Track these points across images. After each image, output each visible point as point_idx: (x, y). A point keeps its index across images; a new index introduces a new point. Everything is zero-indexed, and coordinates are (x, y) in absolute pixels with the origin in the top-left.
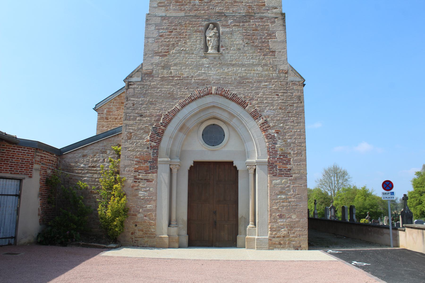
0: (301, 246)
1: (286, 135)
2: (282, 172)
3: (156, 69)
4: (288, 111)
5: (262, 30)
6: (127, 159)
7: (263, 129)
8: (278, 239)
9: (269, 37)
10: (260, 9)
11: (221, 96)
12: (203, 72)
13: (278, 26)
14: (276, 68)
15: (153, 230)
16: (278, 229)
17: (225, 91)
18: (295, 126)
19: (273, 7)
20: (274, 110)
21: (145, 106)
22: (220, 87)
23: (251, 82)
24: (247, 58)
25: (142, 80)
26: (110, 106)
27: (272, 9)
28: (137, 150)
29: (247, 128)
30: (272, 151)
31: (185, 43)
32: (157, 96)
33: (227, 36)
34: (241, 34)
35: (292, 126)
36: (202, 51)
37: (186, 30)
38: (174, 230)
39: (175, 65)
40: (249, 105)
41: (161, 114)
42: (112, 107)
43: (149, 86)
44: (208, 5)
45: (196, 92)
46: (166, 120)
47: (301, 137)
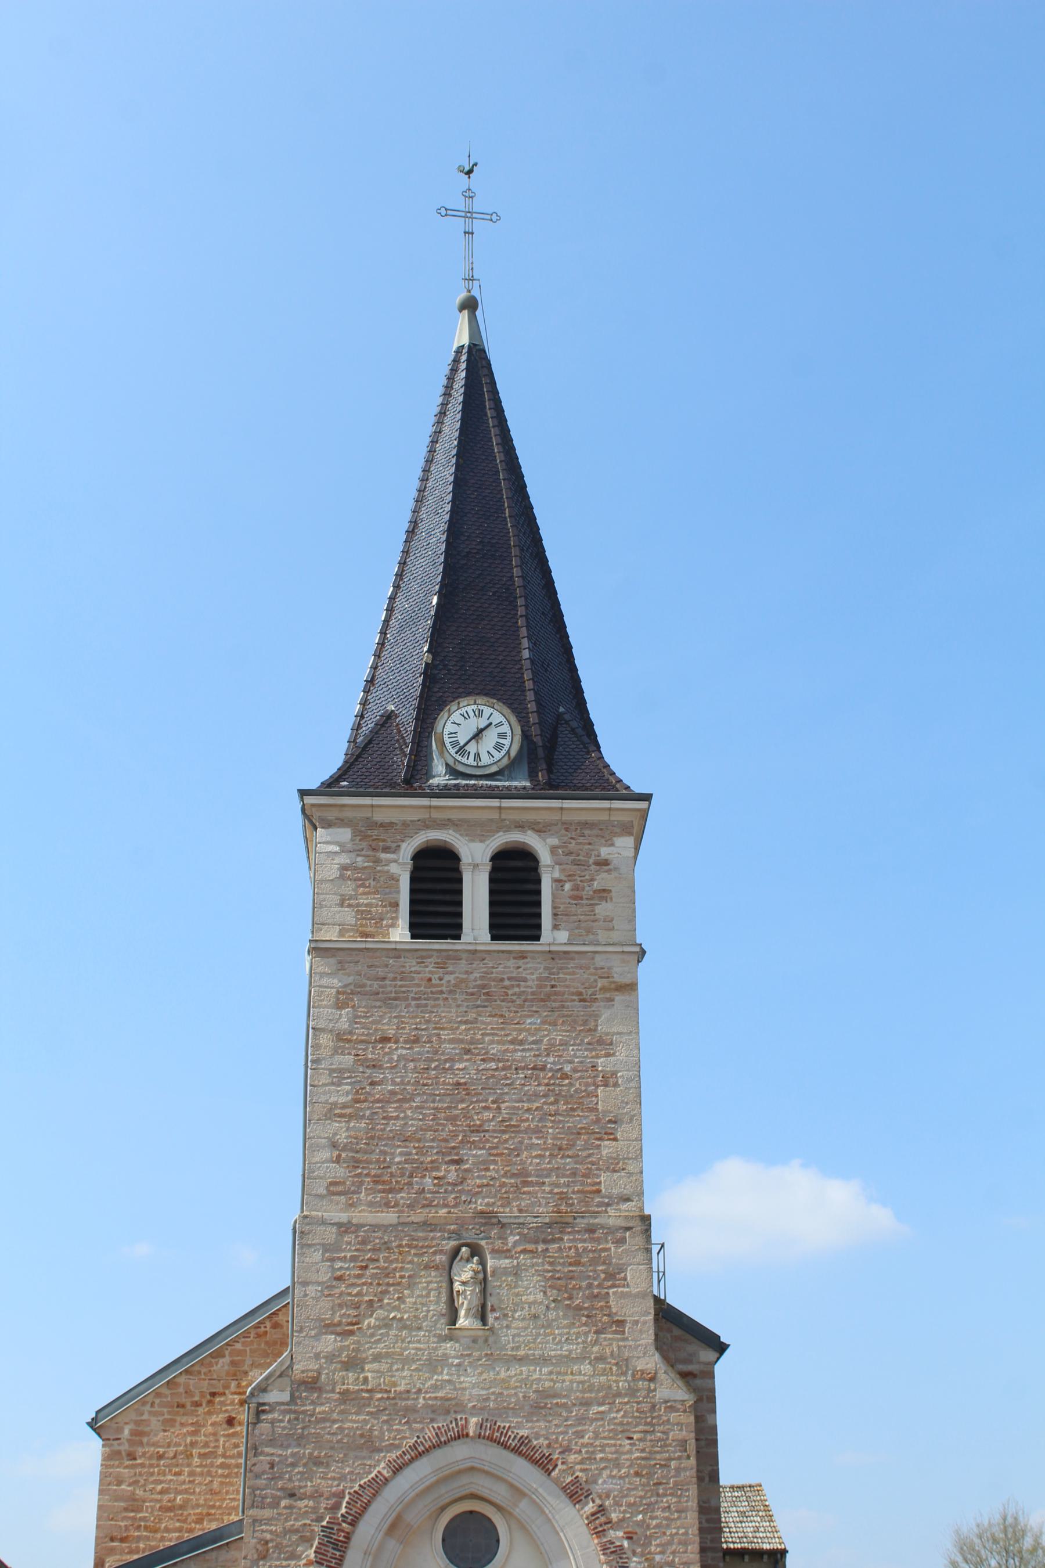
1: (651, 1544)
3: (328, 1369)
4: (655, 1481)
5: (594, 1262)
7: (594, 1529)
9: (610, 1283)
11: (490, 1443)
12: (446, 1377)
13: (633, 1251)
17: (501, 1430)
18: (674, 1519)
19: (621, 1197)
20: (621, 1478)
21: (301, 1469)
22: (487, 1420)
24: (554, 1339)
26: (142, 1414)
27: (618, 1203)
29: (556, 1525)
31: (399, 1298)
34: (539, 1275)
35: (666, 1518)
37: (403, 1262)
39: (377, 1358)
40: (560, 1467)
41: (343, 1491)
42: (149, 1420)
43: (312, 1415)
44: (457, 1192)
45: (428, 1432)
46: (353, 1506)
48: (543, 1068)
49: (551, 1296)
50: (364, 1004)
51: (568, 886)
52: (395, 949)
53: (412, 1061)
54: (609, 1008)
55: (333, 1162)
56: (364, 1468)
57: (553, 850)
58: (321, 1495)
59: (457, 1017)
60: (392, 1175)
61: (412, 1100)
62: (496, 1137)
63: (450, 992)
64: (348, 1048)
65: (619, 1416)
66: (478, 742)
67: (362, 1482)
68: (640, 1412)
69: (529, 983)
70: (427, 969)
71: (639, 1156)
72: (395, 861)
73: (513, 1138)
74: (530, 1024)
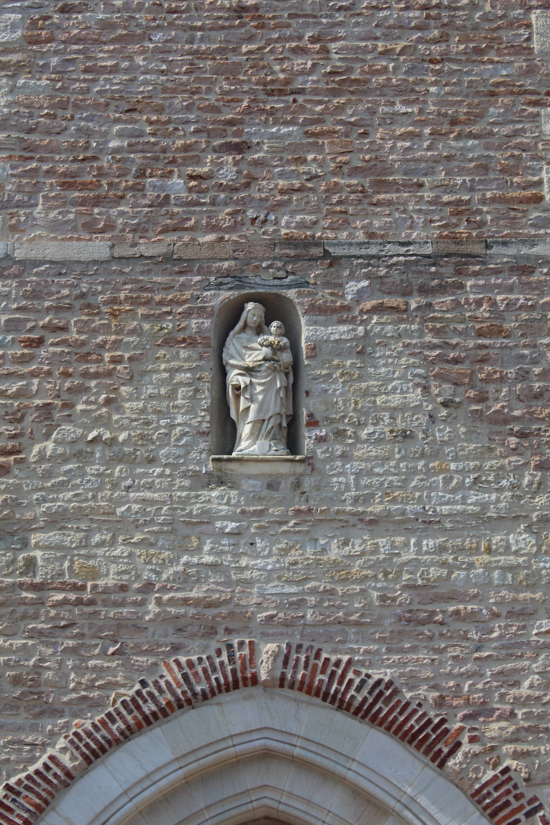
10: (513, 222)
12: (208, 559)
17: (331, 668)
22: (300, 647)
23: (473, 612)
31: (108, 402)
33: (338, 366)
34: (411, 355)
37: (117, 333)
40: (466, 747)
44: (237, 203)
45: (165, 673)
49: (438, 395)
56: (20, 750)
60: (101, 173)
61: (146, 36)
62: (320, 103)
67: (12, 781)
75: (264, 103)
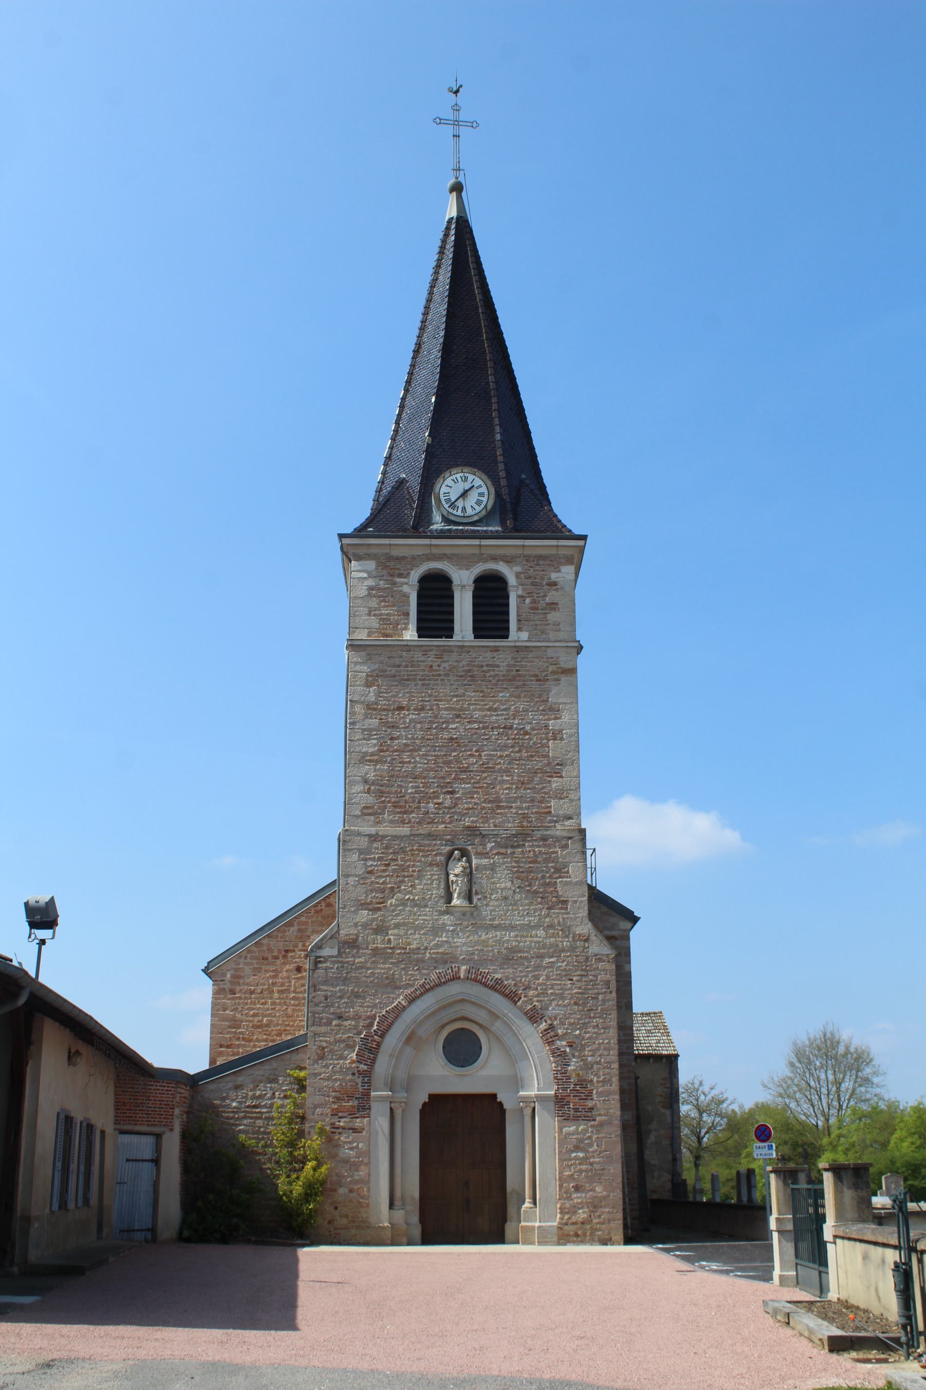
0: (610, 1239)
2: (579, 1113)
3: (364, 933)
6: (317, 1093)
7: (546, 1040)
8: (572, 1228)
9: (557, 875)
10: (542, 821)
11: (474, 983)
12: (445, 939)
14: (569, 931)
15: (365, 1215)
16: (573, 1210)
17: (483, 974)
18: (601, 1033)
19: (565, 817)
20: (564, 1006)
21: (346, 1000)
22: (473, 967)
23: (526, 956)
25: (340, 954)
26: (239, 964)
27: (563, 821)
28: (335, 1077)
29: (520, 1038)
30: (561, 1077)
31: (411, 886)
32: (367, 982)
34: (508, 870)
35: (595, 1033)
36: (442, 901)
38: (399, 1214)
39: (397, 926)
41: (375, 1015)
43: (353, 965)
44: (451, 813)
47: (609, 1053)
48: (511, 728)
50: (385, 683)
51: (528, 601)
52: (407, 645)
53: (419, 723)
54: (557, 686)
55: (365, 793)
56: (389, 1000)
57: (518, 575)
58: (360, 1018)
59: (451, 692)
60: (406, 802)
62: (479, 775)
63: (446, 675)
64: (375, 714)
65: (563, 965)
66: (464, 499)
67: (388, 1009)
68: (578, 962)
69: (501, 669)
70: (430, 659)
71: (578, 788)
72: (407, 584)
73: (490, 776)
74: (502, 697)
75: (460, 775)
